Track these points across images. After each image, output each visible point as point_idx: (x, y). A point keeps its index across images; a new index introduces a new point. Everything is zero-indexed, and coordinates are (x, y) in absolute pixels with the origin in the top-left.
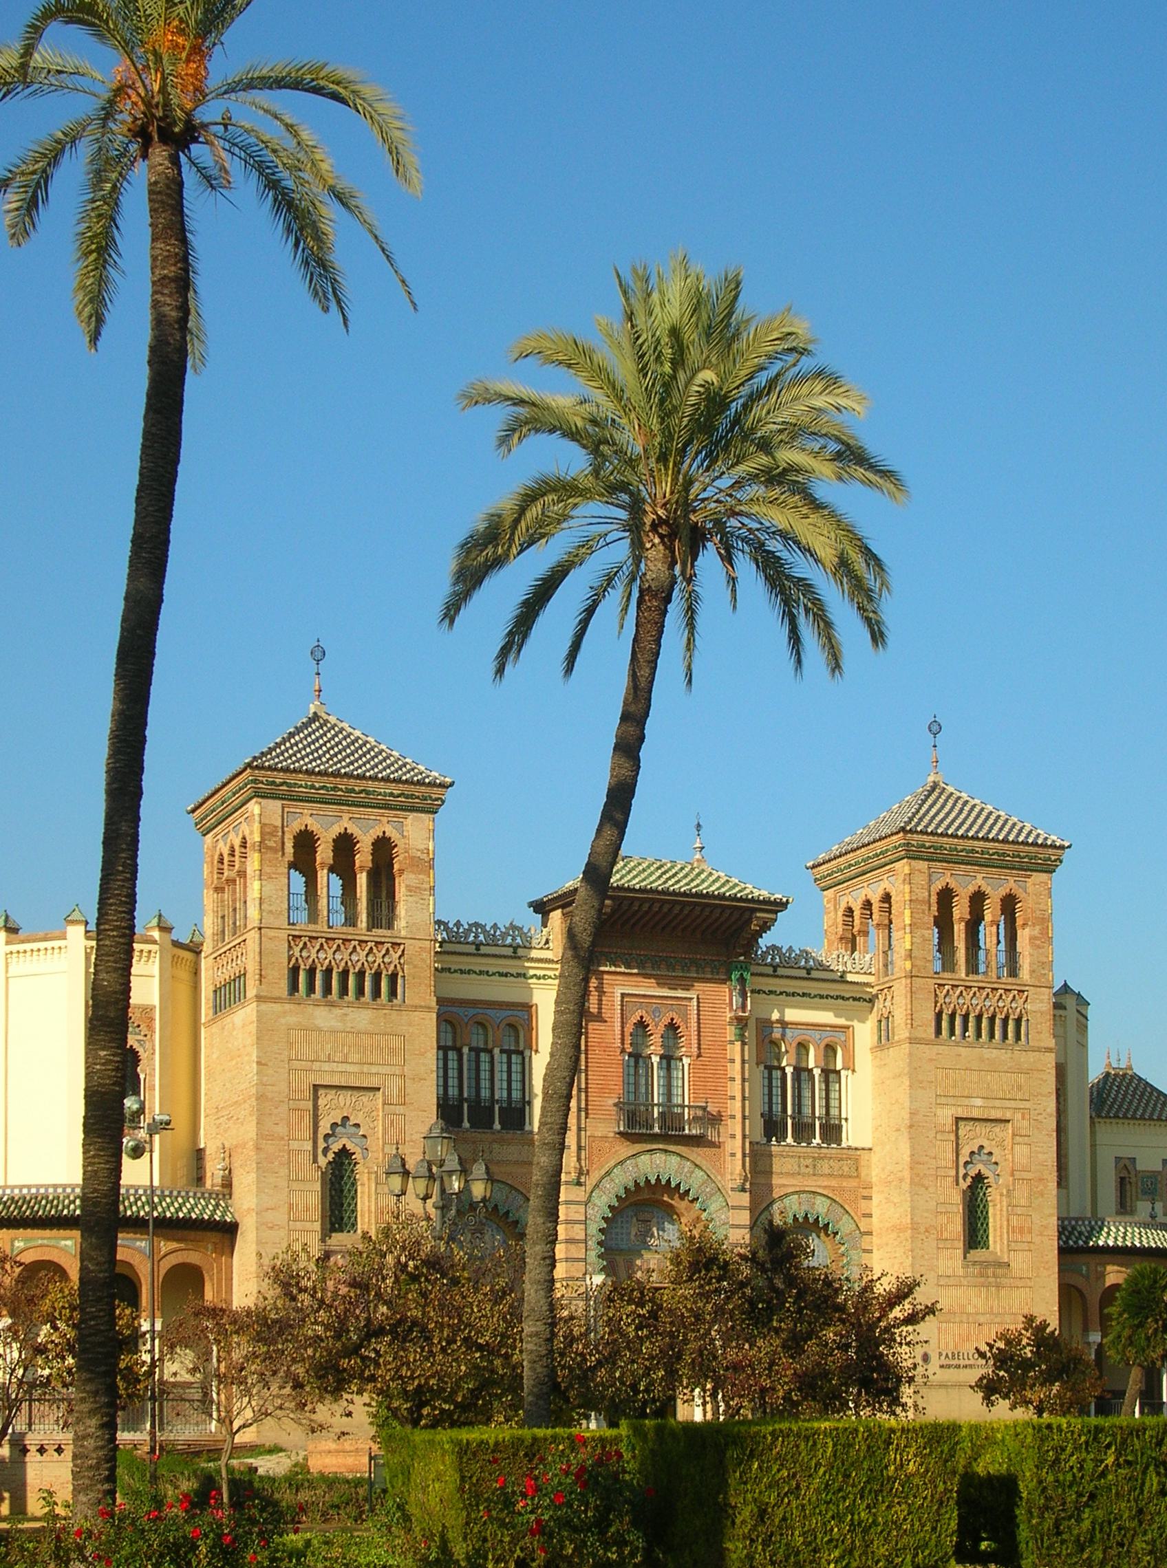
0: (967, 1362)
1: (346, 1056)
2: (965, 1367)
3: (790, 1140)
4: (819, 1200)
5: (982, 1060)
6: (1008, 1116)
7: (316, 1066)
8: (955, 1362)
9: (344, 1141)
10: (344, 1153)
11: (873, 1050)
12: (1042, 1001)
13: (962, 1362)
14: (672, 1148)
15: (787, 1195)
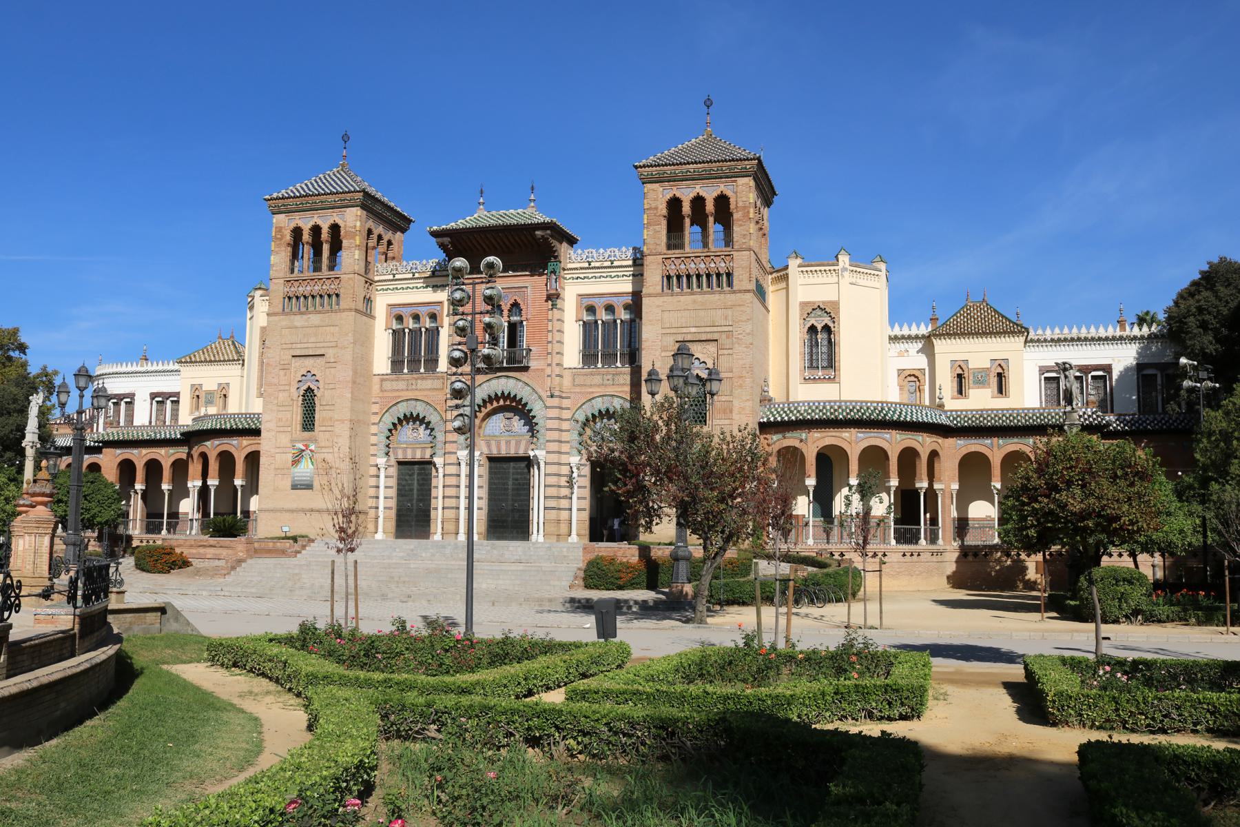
5: (694, 301)
6: (716, 336)
10: (309, 389)
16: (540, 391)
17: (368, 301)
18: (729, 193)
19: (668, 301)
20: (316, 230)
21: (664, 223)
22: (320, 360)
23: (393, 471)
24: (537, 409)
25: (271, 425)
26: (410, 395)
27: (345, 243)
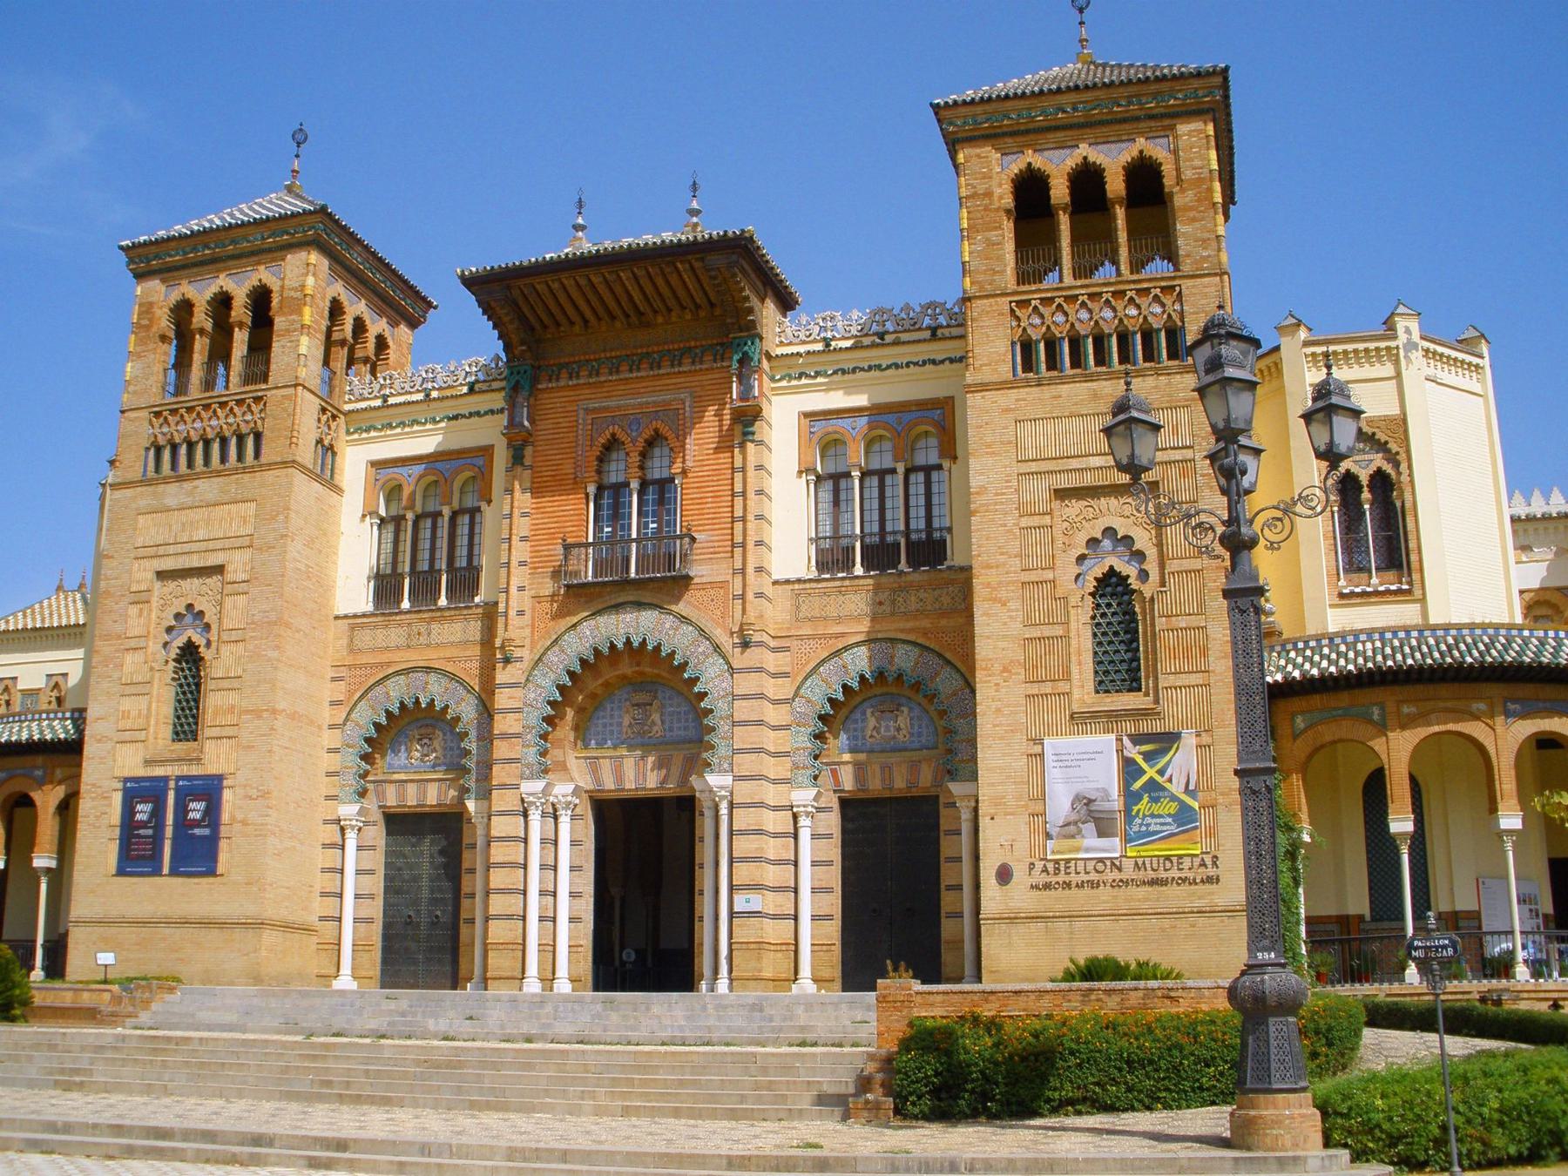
0: (1086, 878)
2: (1080, 886)
4: (901, 650)
7: (161, 551)
8: (1061, 878)
12: (1206, 296)
13: (1074, 878)
15: (846, 649)
17: (327, 450)
18: (1157, 150)
19: (1030, 398)
20: (223, 302)
21: (1008, 226)
23: (377, 834)
24: (711, 676)
27: (280, 322)
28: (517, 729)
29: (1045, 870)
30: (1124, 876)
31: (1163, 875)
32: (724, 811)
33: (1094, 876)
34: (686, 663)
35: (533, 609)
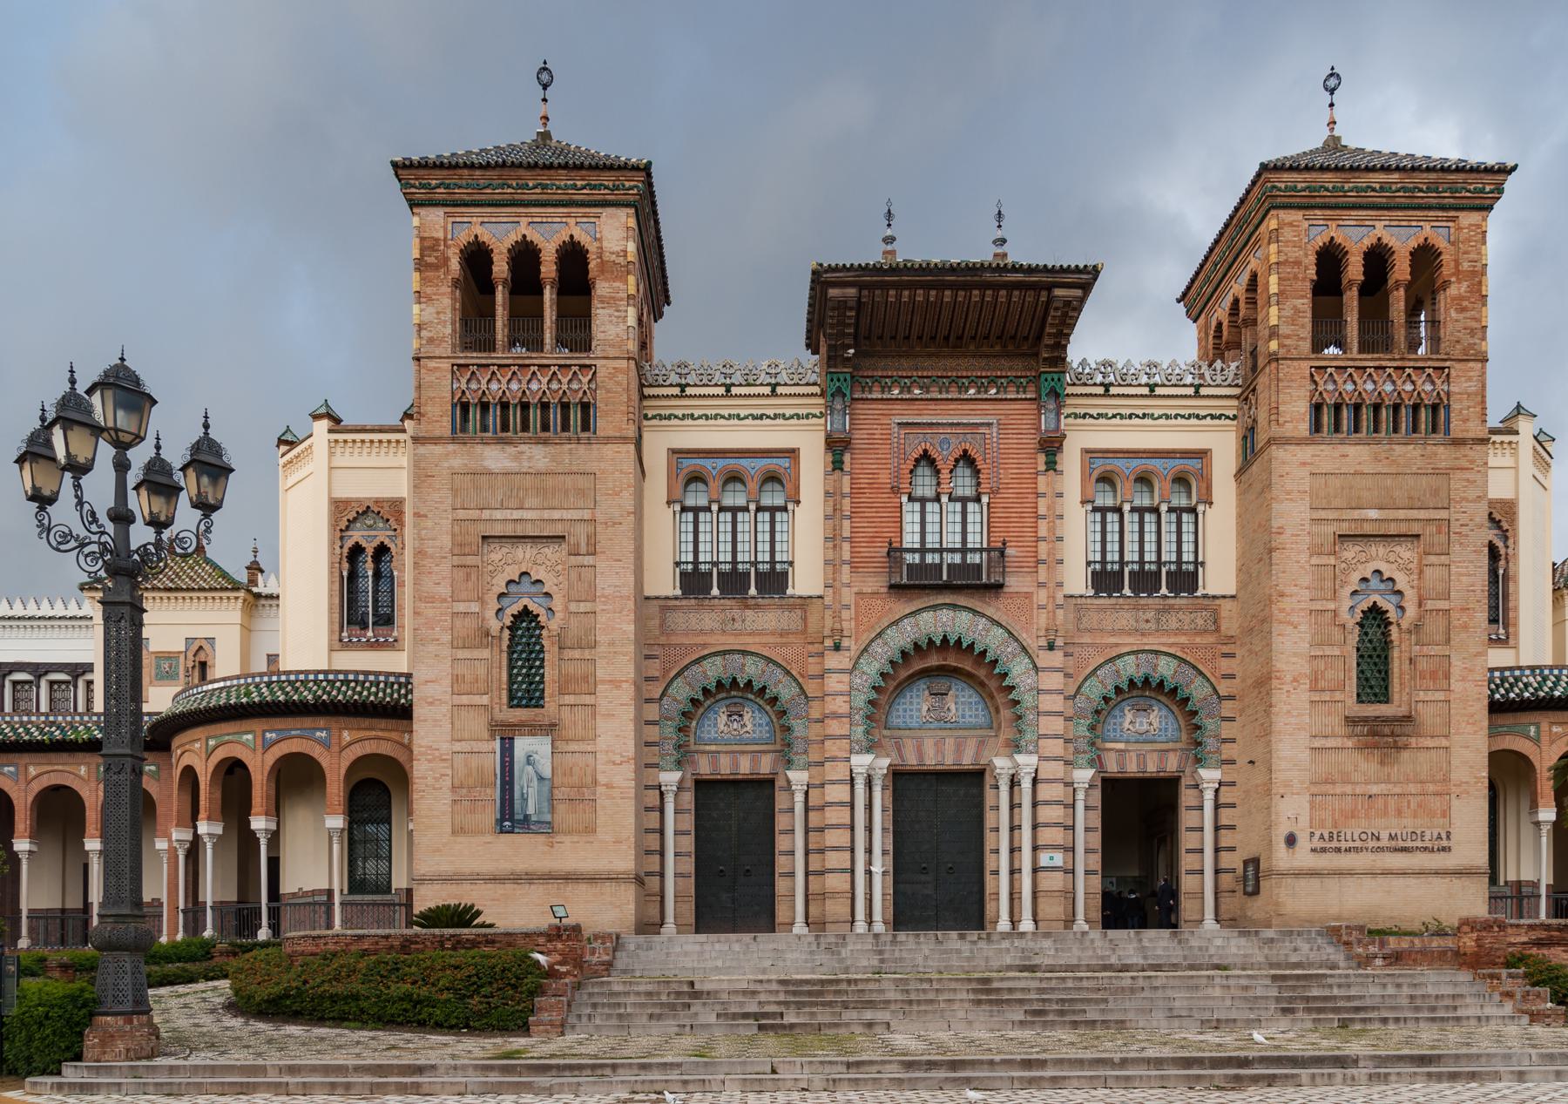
0: (1351, 844)
1: (522, 502)
2: (1348, 850)
3: (1127, 591)
8: (1335, 844)
9: (525, 601)
10: (525, 613)
11: (1240, 472)
13: (1343, 845)
14: (962, 600)
16: (1023, 636)
22: (550, 552)
24: (1019, 671)
25: (441, 690)
26: (731, 642)
28: (845, 709)
29: (1322, 837)
30: (1380, 844)
31: (1409, 844)
32: (1026, 784)
33: (1358, 844)
34: (996, 661)
35: (857, 605)
